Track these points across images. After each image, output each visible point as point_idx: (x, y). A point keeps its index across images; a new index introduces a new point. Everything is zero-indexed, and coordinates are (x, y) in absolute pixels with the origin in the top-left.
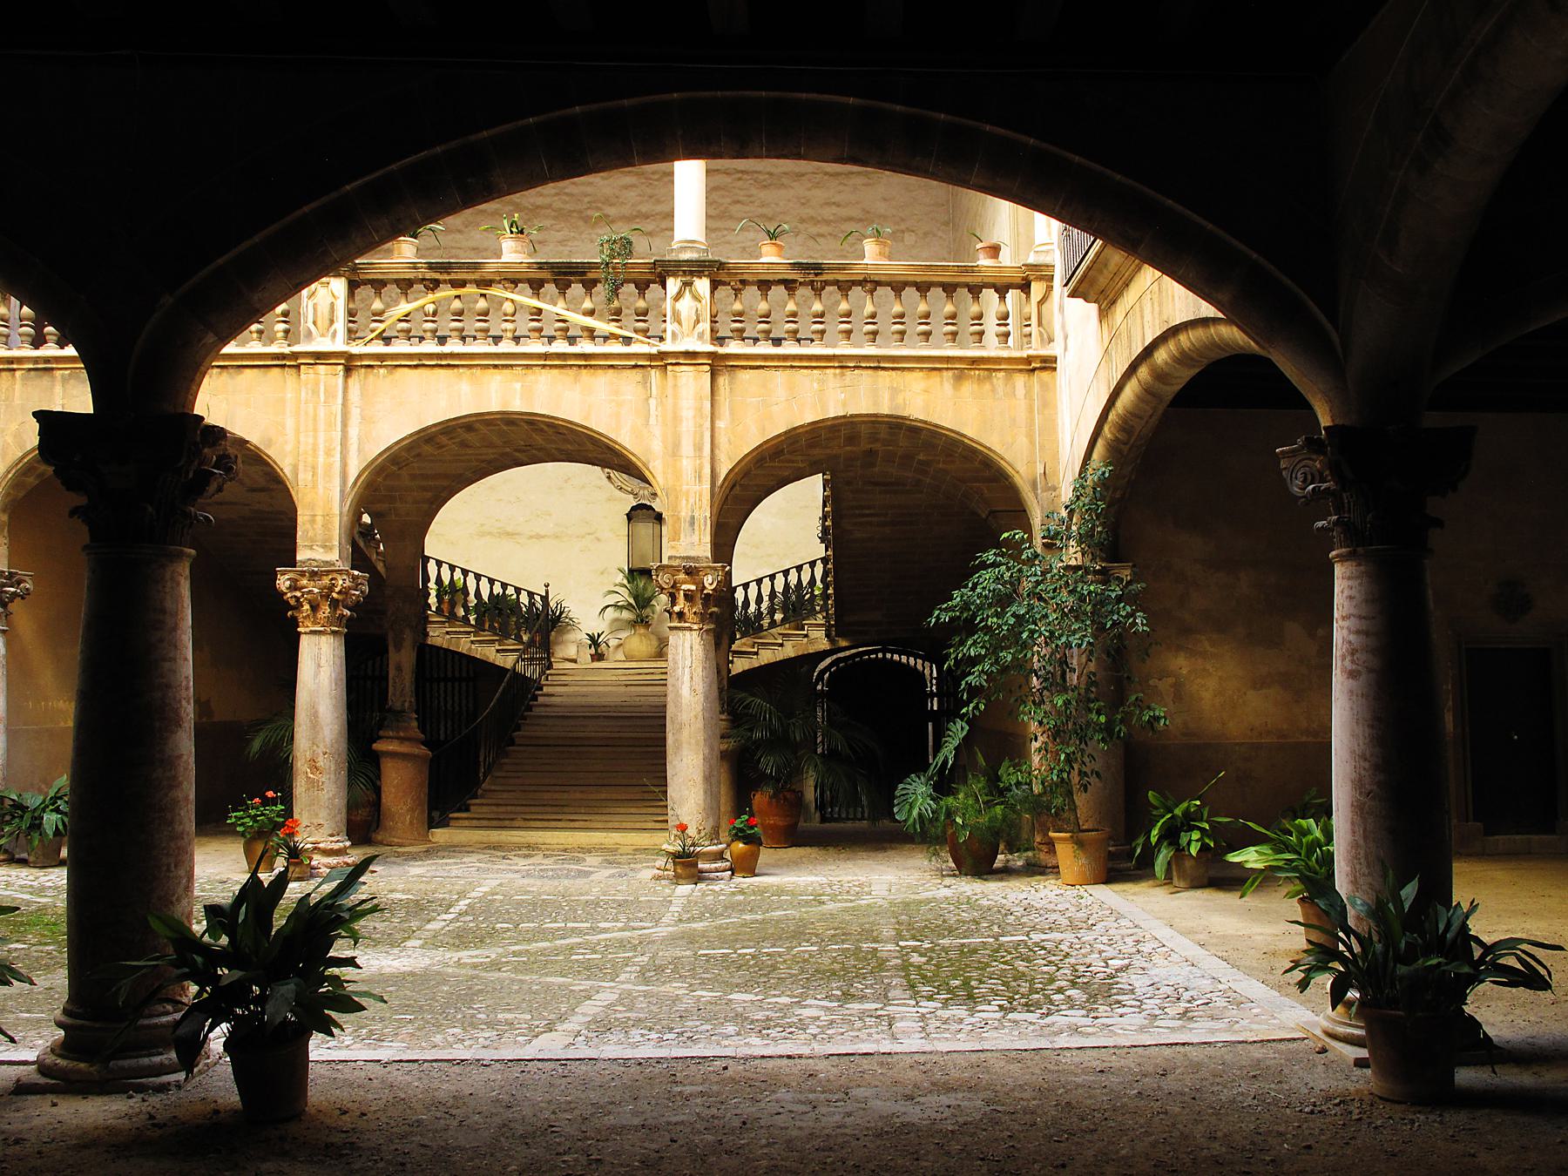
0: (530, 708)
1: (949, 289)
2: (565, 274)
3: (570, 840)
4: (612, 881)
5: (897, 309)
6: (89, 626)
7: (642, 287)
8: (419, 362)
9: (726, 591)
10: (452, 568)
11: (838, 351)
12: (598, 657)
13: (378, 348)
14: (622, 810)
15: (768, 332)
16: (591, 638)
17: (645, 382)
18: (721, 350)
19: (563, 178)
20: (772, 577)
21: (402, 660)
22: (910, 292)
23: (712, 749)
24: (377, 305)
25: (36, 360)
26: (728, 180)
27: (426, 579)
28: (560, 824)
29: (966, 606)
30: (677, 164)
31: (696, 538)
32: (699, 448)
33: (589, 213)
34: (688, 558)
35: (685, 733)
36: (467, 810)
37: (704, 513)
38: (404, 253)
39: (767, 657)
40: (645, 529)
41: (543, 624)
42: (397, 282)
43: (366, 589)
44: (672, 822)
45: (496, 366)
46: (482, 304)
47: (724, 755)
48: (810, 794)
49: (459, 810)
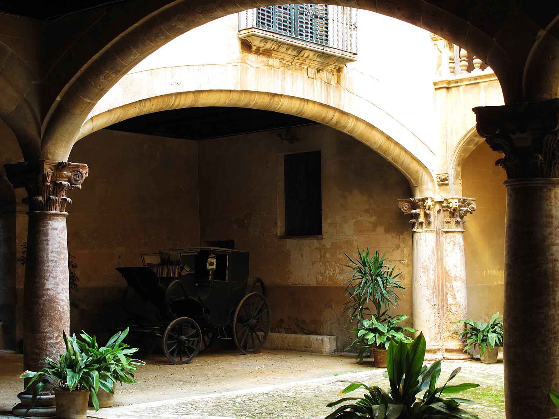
6: (510, 226)
25: (470, 79)
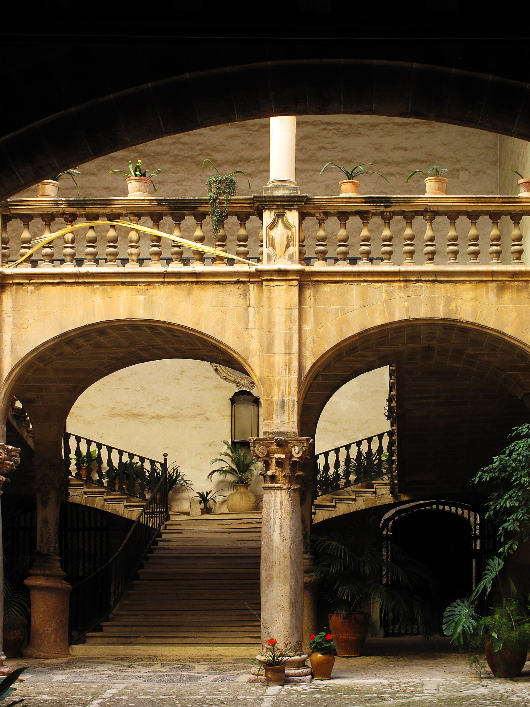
0: (151, 551)
1: (495, 216)
2: (180, 208)
3: (183, 653)
4: (216, 684)
5: (452, 233)
7: (243, 218)
8: (60, 280)
9: (310, 457)
10: (89, 442)
11: (403, 268)
12: (207, 510)
13: (27, 269)
14: (225, 629)
15: (345, 254)
16: (201, 495)
17: (245, 295)
18: (307, 269)
19: (176, 132)
20: (348, 447)
21: (47, 516)
22: (463, 220)
23: (297, 582)
24: (26, 234)
26: (315, 130)
27: (68, 451)
28: (175, 640)
29: (503, 468)
30: (271, 118)
31: (285, 418)
32: (288, 346)
33: (200, 158)
34: (279, 433)
35: (276, 569)
36: (101, 630)
37: (292, 397)
38: (48, 193)
39: (342, 509)
40: (245, 410)
41: (163, 485)
42: (43, 216)
43: (18, 459)
44: (265, 638)
45: (123, 283)
46: (112, 233)
47: (307, 586)
48: (376, 615)
49: (94, 630)
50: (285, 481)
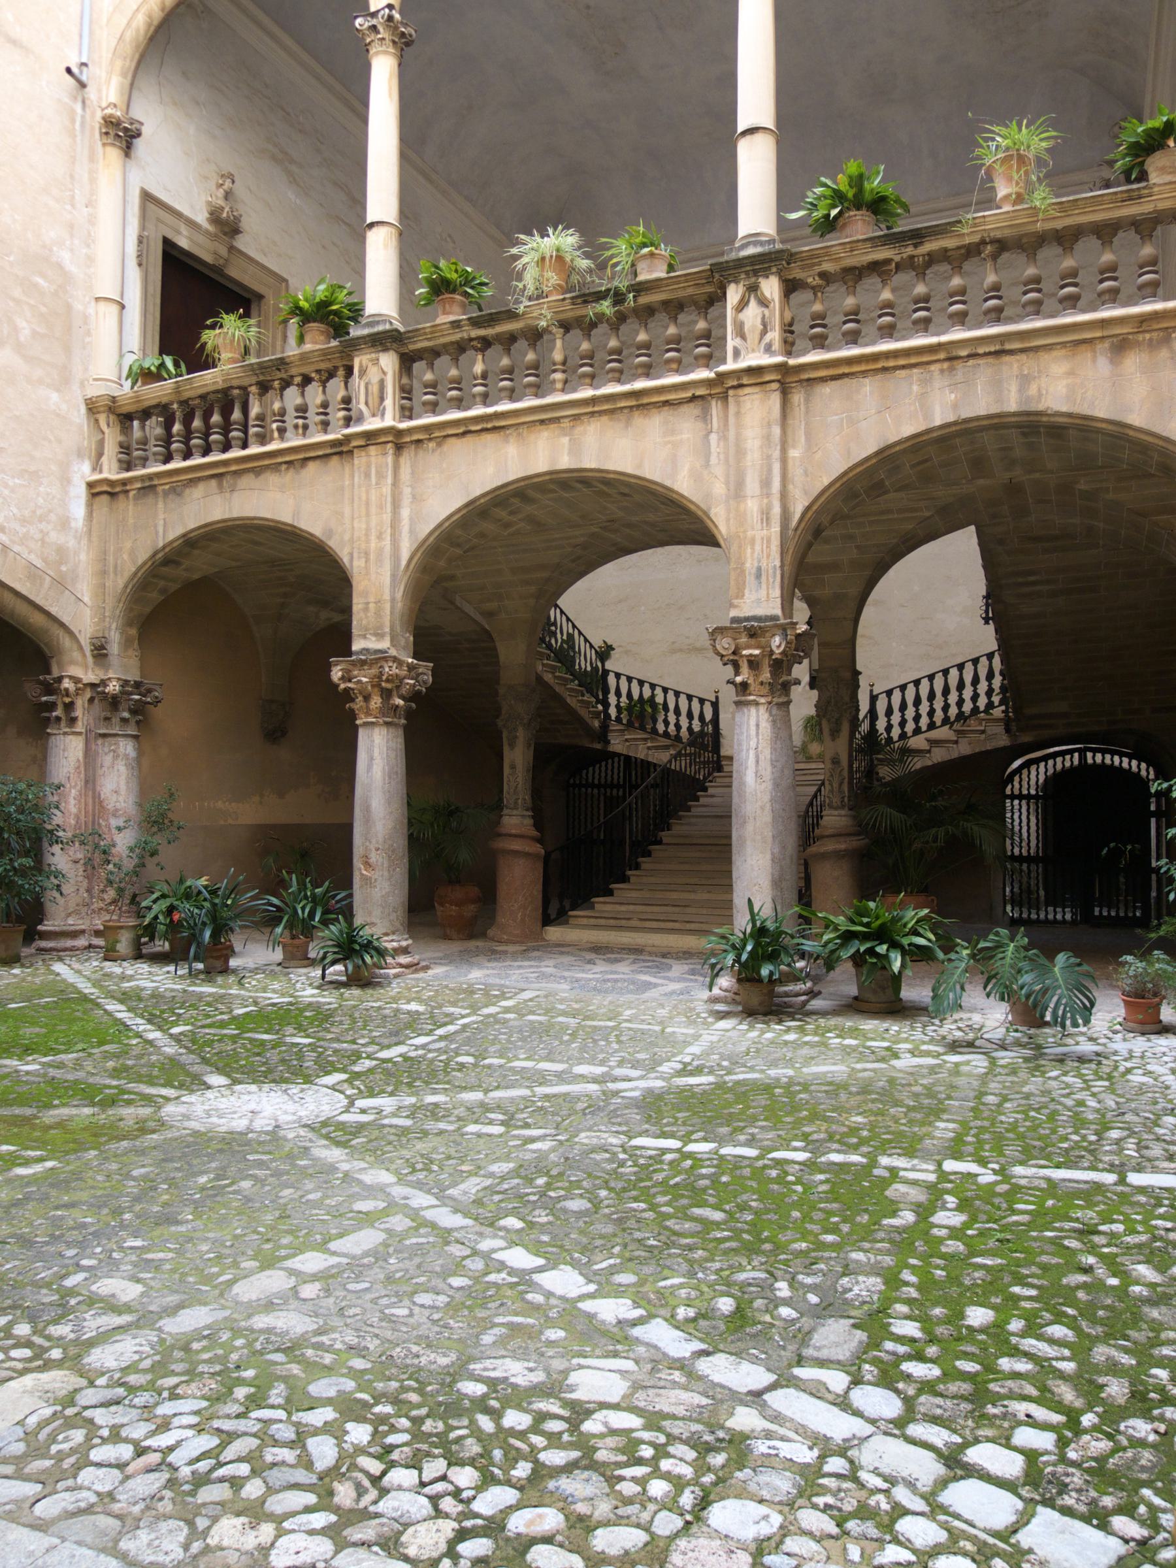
8: (465, 430)
17: (705, 417)
18: (792, 362)
32: (766, 483)
45: (542, 422)
50: (765, 690)
